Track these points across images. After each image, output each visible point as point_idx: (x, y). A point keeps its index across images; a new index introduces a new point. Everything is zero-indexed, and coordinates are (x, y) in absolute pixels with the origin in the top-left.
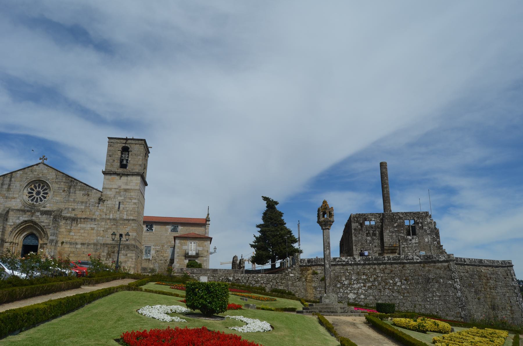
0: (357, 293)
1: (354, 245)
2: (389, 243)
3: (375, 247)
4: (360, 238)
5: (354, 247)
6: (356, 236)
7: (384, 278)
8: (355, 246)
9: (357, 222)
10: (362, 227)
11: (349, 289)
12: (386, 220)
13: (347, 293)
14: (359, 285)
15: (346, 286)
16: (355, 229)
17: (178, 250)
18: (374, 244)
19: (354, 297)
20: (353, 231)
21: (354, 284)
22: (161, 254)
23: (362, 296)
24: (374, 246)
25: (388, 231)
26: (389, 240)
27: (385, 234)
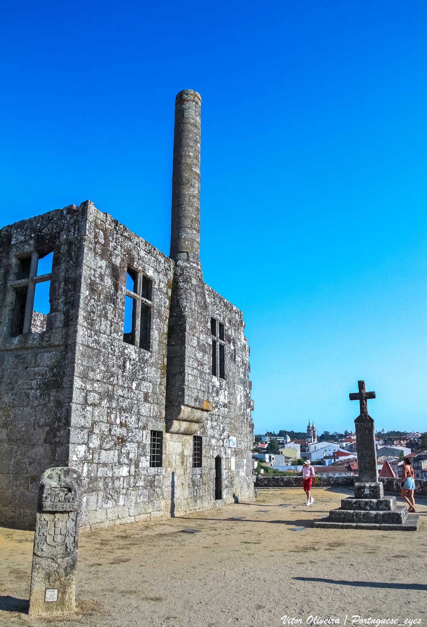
1: (78, 369)
5: (78, 383)
8: (84, 377)
9: (105, 254)
20: (85, 292)
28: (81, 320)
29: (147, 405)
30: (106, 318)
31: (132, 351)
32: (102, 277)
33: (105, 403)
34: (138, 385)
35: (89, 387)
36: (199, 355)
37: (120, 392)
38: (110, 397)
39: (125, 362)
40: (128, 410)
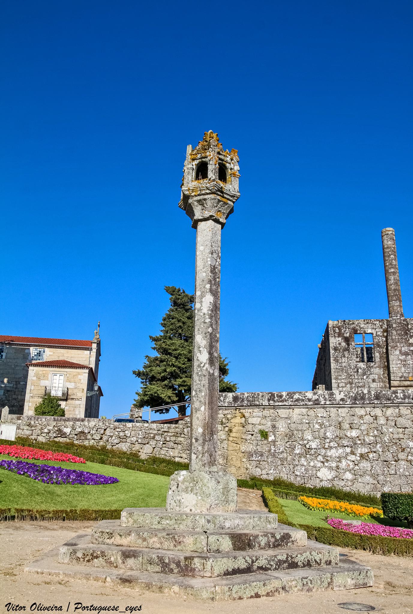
0: (337, 467)
1: (333, 377)
2: (400, 375)
3: (374, 381)
4: (344, 365)
5: (333, 381)
6: (336, 360)
7: (396, 436)
8: (336, 379)
9: (340, 334)
10: (348, 345)
11: (320, 458)
12: (394, 332)
13: (314, 467)
14: (341, 451)
15: (312, 452)
16: (336, 349)
17: (33, 388)
18: (372, 377)
19: (330, 477)
20: (332, 352)
21: (331, 448)
22: (14, 396)
23: (349, 476)
24: (370, 380)
25: (397, 352)
26: (400, 368)
27: (391, 357)
28: (332, 361)
29: (375, 383)
30: (344, 357)
31: (361, 365)
32: (340, 344)
33: (348, 386)
34: (367, 377)
35: (339, 382)
36: (403, 357)
37: (356, 381)
38: (351, 383)
39: (358, 370)
40: (364, 386)
